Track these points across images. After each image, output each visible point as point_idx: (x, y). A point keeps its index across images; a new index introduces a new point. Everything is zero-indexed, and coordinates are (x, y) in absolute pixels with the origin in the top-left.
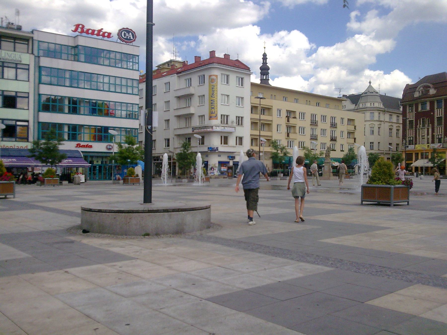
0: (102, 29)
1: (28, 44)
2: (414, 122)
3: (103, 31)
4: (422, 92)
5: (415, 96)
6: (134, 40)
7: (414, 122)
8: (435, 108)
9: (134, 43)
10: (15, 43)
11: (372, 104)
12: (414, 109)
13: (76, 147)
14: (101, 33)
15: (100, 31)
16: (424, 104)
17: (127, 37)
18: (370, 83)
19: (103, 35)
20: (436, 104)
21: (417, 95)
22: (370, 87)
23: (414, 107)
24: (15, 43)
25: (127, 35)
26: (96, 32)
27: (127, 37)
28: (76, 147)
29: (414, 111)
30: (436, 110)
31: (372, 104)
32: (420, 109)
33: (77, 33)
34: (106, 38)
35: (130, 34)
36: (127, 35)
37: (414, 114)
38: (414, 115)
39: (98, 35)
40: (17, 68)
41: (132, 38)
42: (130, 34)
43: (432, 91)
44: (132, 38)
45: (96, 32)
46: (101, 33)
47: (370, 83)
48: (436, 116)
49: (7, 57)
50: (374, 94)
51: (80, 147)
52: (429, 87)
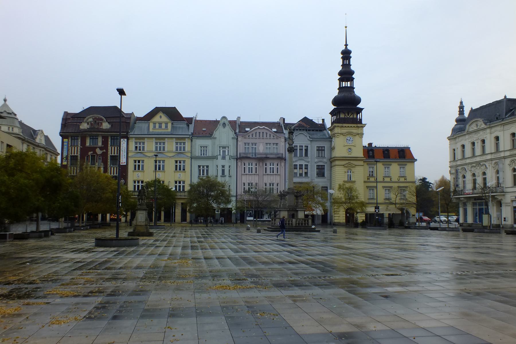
2: (79, 158)
4: (91, 124)
5: (81, 127)
7: (79, 158)
8: (109, 145)
11: (11, 129)
12: (79, 143)
16: (94, 138)
18: (5, 100)
20: (110, 140)
21: (84, 126)
22: (5, 105)
23: (79, 140)
29: (79, 145)
30: (110, 148)
31: (11, 129)
32: (88, 144)
37: (79, 148)
38: (79, 150)
43: (106, 125)
47: (5, 100)
48: (109, 154)
50: (13, 116)
52: (102, 120)
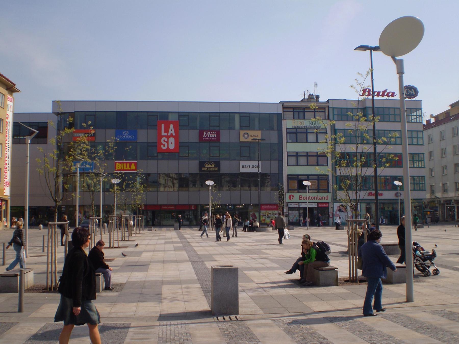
0: (386, 90)
1: (325, 112)
3: (388, 91)
6: (417, 96)
9: (417, 98)
13: (369, 195)
14: (386, 94)
15: (384, 92)
17: (410, 93)
19: (388, 95)
25: (410, 91)
26: (381, 94)
27: (410, 93)
28: (369, 195)
33: (365, 97)
34: (390, 98)
35: (413, 90)
36: (410, 91)
39: (383, 95)
41: (414, 94)
42: (413, 90)
44: (414, 94)
45: (381, 94)
46: (386, 94)
49: (309, 125)
51: (371, 195)
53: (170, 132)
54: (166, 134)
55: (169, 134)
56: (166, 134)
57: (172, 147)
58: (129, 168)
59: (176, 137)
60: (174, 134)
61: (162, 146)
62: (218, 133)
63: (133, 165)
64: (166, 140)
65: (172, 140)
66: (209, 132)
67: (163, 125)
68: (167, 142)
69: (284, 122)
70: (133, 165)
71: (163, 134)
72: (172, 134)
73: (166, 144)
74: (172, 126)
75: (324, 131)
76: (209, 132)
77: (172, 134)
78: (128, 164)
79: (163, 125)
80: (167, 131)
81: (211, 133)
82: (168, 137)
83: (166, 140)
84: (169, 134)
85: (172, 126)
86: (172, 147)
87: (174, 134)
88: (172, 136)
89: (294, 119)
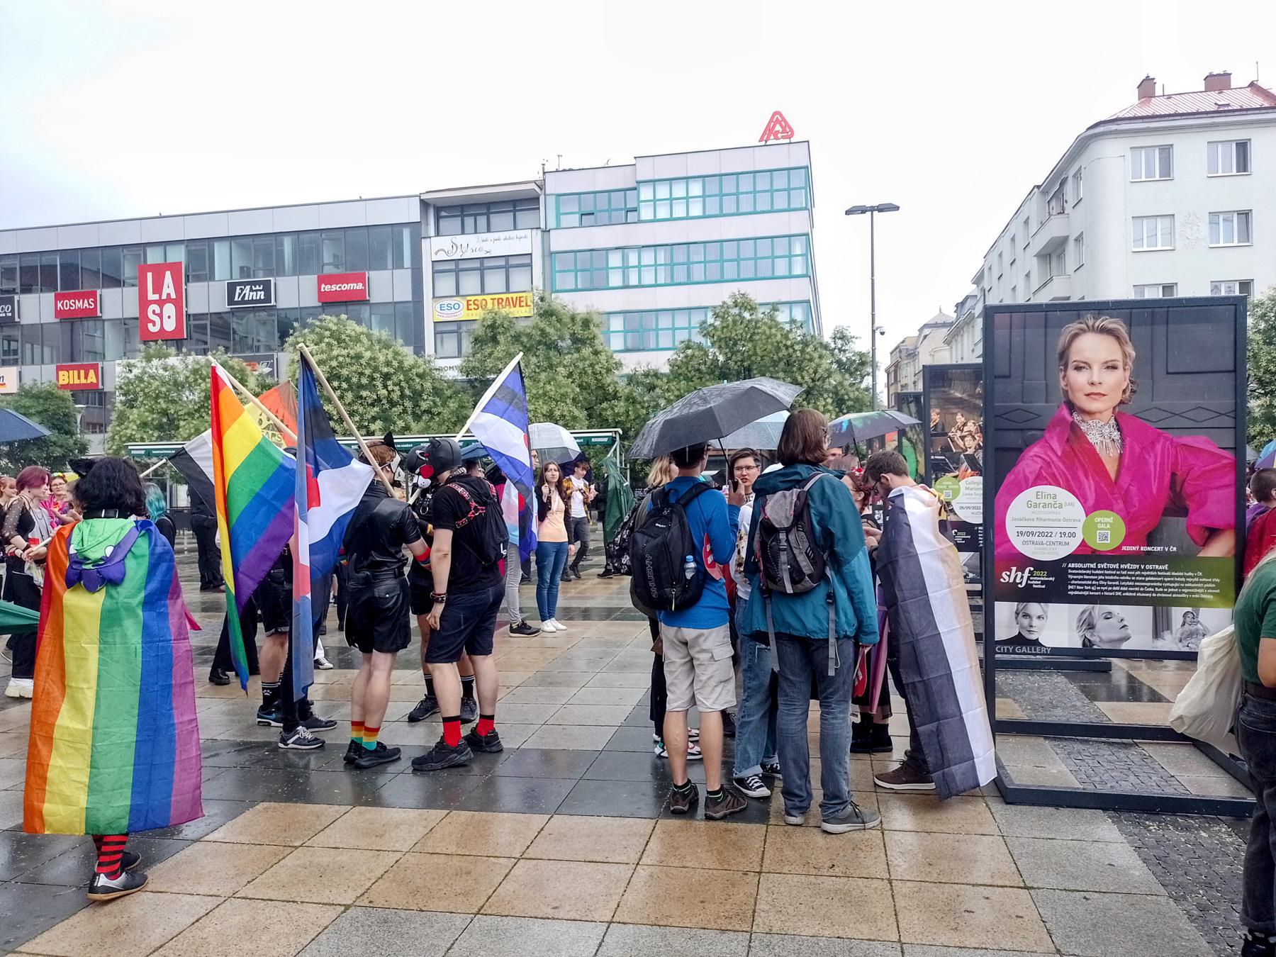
10: (514, 211)
24: (514, 211)
40: (507, 268)
53: (165, 291)
54: (156, 297)
55: (164, 297)
56: (156, 297)
57: (170, 325)
58: (83, 381)
59: (177, 303)
60: (173, 296)
61: (150, 326)
62: (266, 286)
63: (92, 372)
64: (158, 311)
65: (169, 309)
66: (248, 287)
67: (150, 275)
68: (160, 315)
69: (425, 243)
70: (92, 372)
71: (152, 296)
72: (168, 295)
73: (157, 319)
74: (168, 274)
75: (526, 260)
76: (248, 287)
77: (168, 295)
78: (82, 372)
79: (150, 275)
80: (158, 288)
81: (251, 290)
82: (161, 303)
83: (158, 311)
84: (164, 297)
85: (168, 274)
86: (170, 325)
87: (173, 296)
88: (169, 300)
89: (463, 233)
